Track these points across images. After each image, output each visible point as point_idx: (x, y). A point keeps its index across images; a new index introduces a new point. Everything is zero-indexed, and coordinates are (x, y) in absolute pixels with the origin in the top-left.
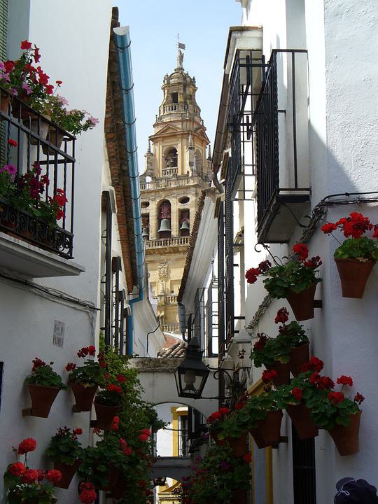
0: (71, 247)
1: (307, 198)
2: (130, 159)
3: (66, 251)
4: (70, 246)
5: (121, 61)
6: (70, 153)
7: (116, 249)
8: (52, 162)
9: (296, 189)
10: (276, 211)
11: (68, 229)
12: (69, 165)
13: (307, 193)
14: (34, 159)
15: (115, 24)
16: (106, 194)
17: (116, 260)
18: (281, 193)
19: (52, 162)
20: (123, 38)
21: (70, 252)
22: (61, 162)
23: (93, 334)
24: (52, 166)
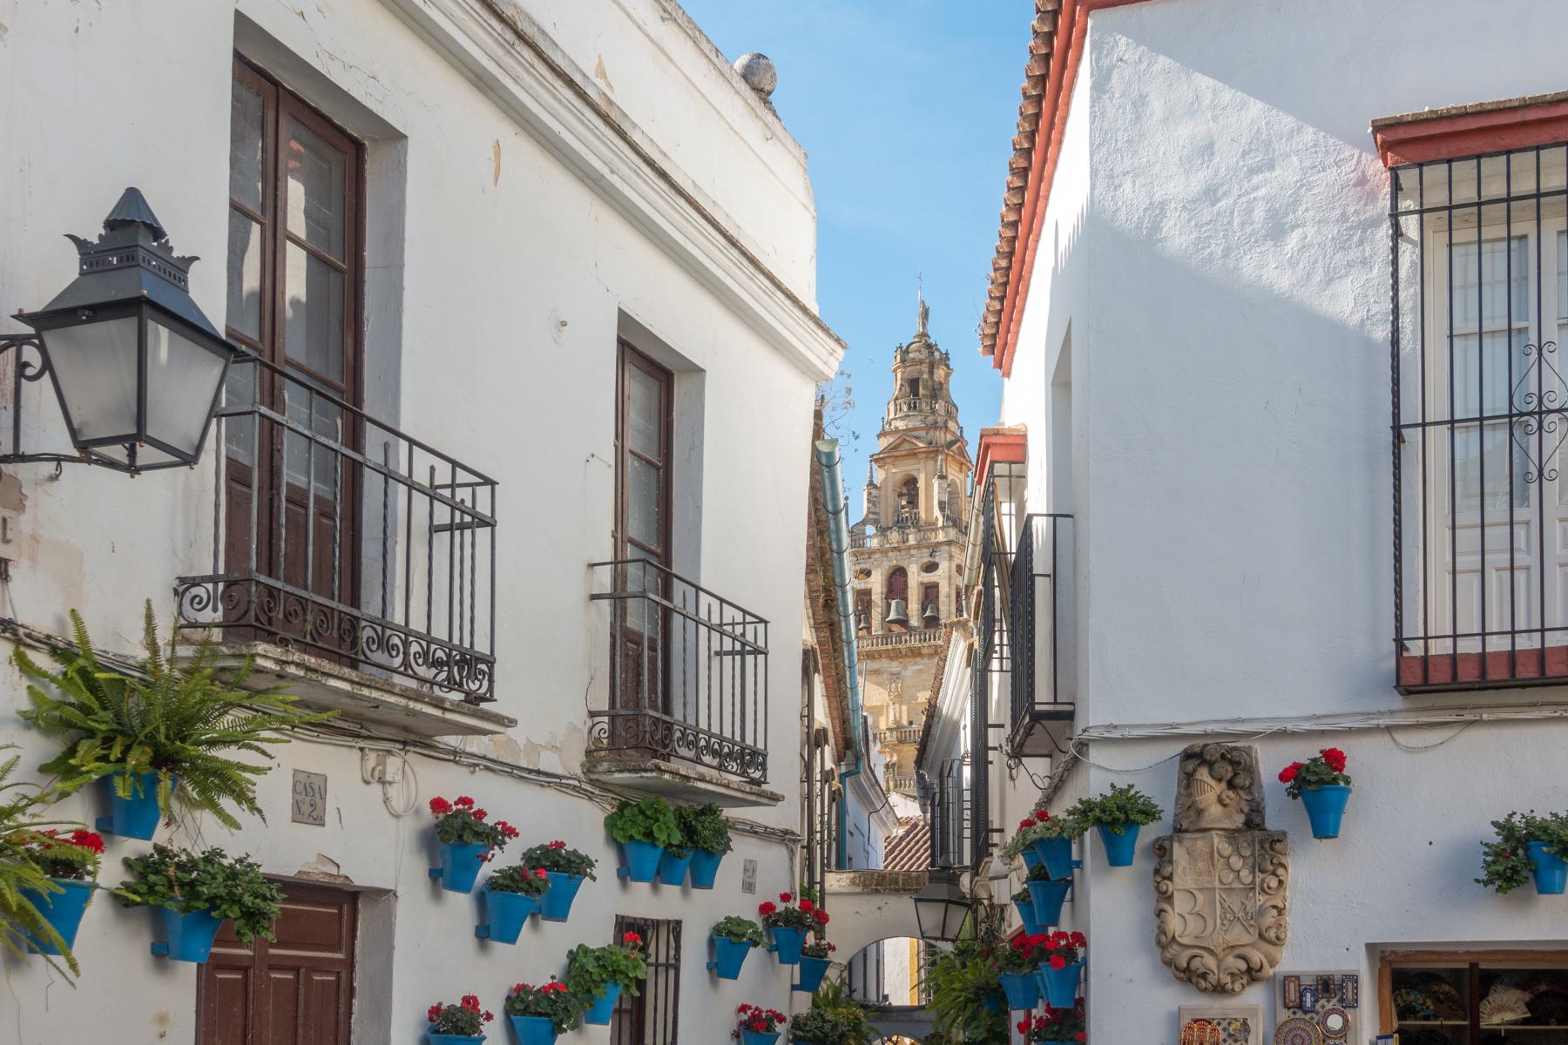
0: (765, 770)
1: (1070, 716)
2: (836, 563)
3: (757, 775)
4: (763, 766)
5: (828, 486)
6: (761, 643)
7: (822, 717)
8: (738, 653)
9: (1055, 703)
10: (1028, 733)
11: (760, 746)
12: (761, 658)
13: (1070, 708)
14: (715, 646)
15: (818, 433)
16: (808, 654)
17: (823, 733)
18: (1037, 707)
19: (738, 653)
20: (830, 455)
21: (764, 775)
22: (749, 653)
23: (792, 872)
24: (738, 658)
